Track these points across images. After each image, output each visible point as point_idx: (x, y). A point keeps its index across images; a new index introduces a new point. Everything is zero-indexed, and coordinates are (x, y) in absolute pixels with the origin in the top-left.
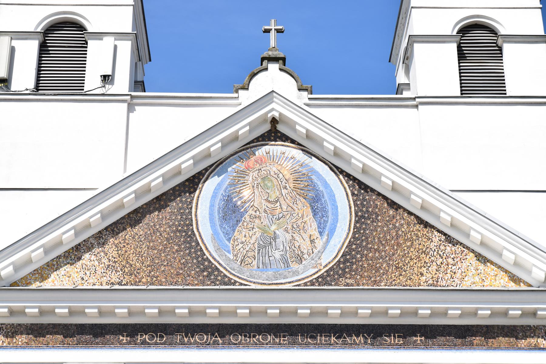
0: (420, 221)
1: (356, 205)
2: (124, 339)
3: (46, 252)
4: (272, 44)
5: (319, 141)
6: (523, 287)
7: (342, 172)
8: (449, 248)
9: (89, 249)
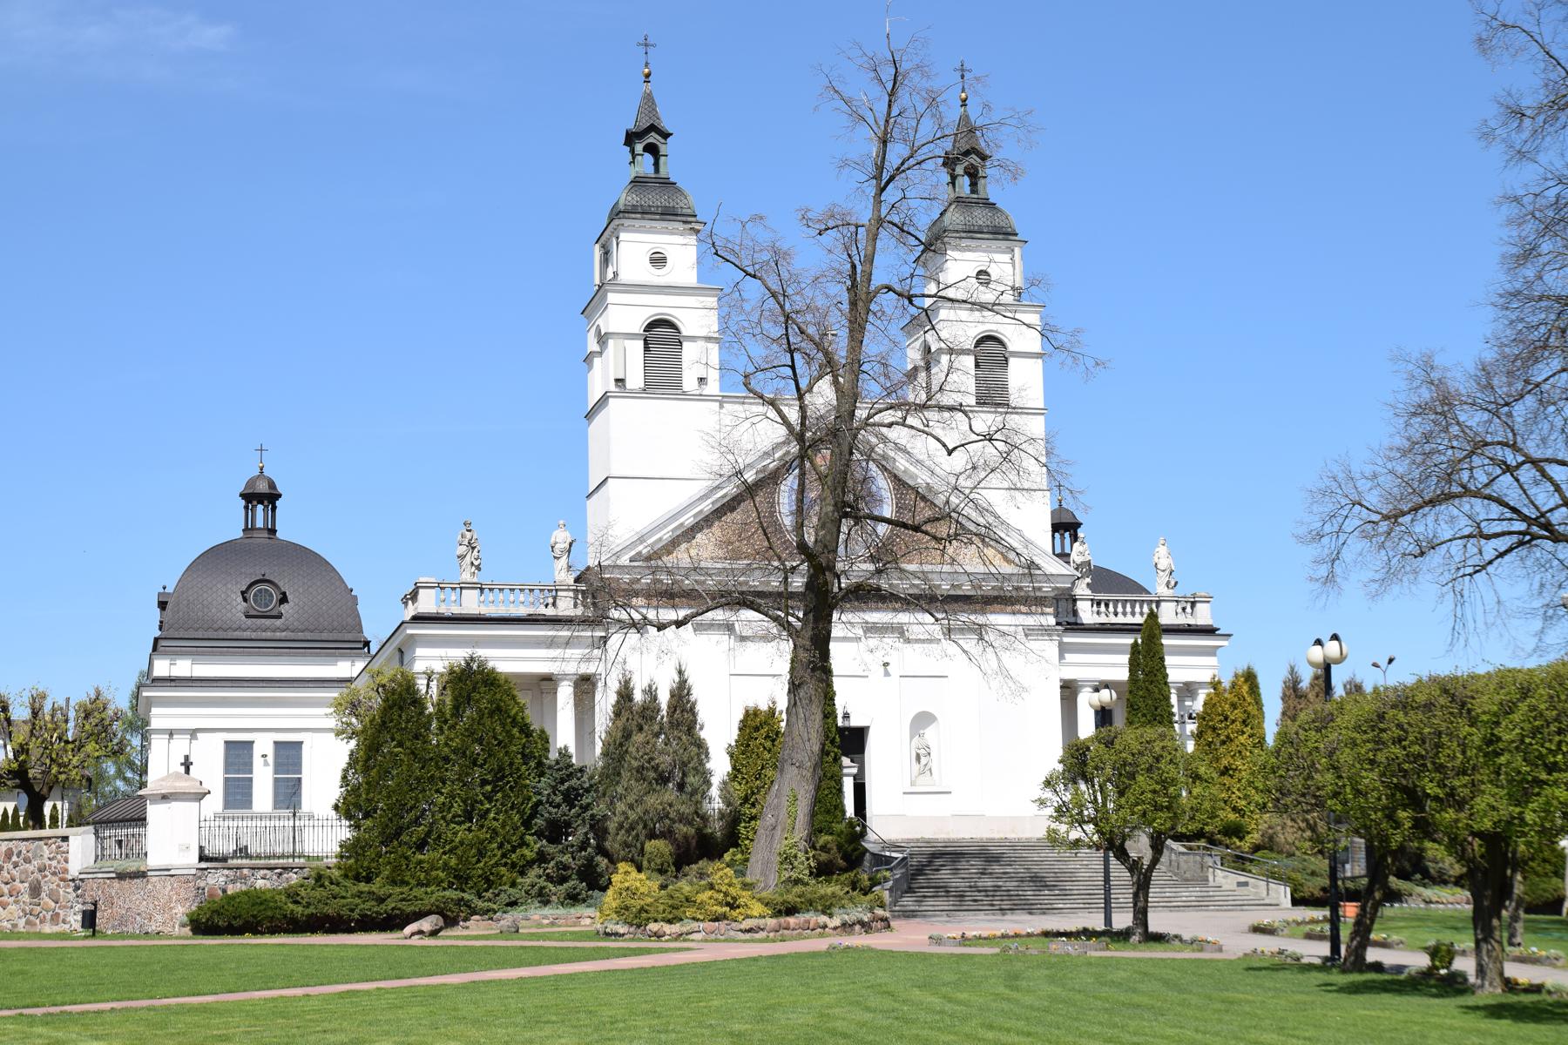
1: (896, 498)
9: (701, 530)
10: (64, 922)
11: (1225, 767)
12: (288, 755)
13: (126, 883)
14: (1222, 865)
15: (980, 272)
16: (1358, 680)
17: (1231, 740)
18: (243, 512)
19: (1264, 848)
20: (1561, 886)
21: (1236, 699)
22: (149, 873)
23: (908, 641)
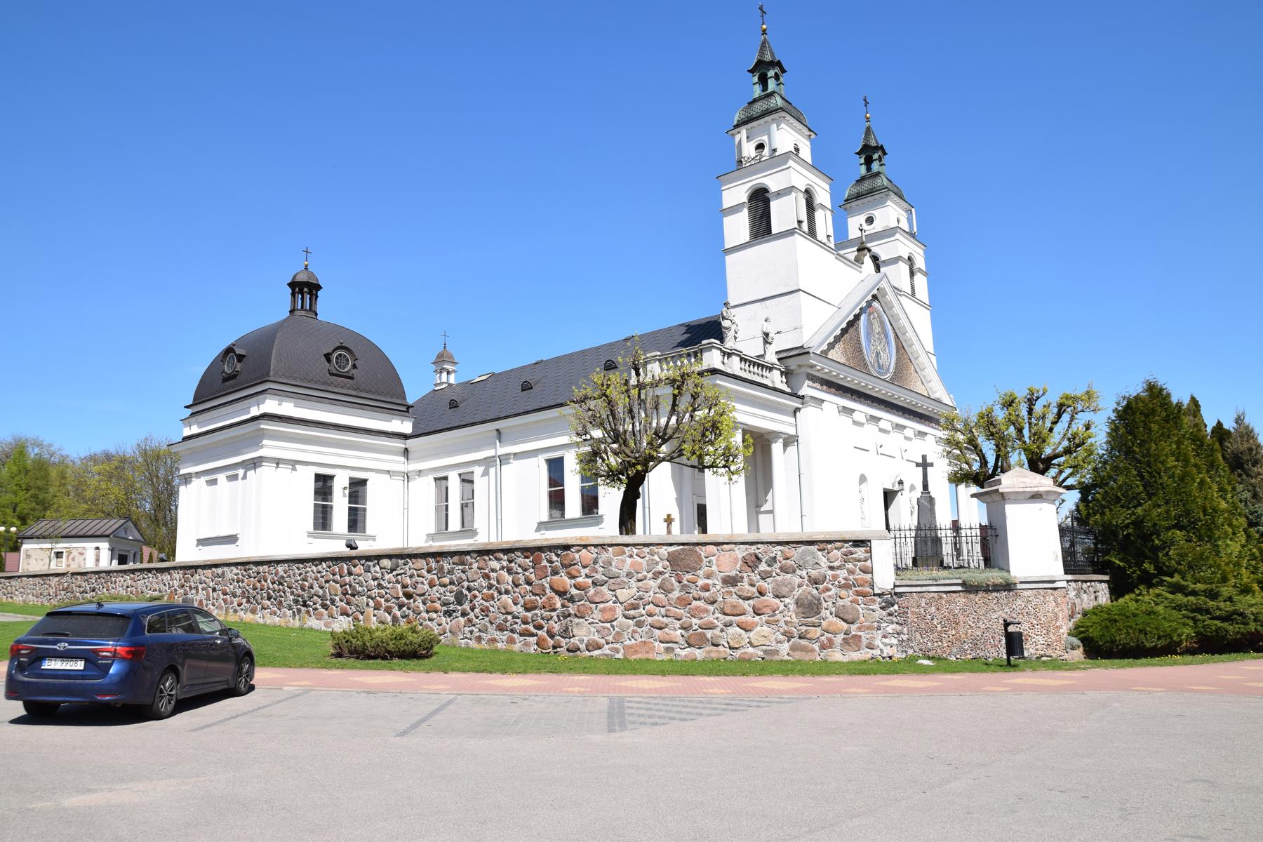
10: (870, 647)
12: (357, 488)
13: (978, 598)
18: (290, 297)
22: (1019, 586)
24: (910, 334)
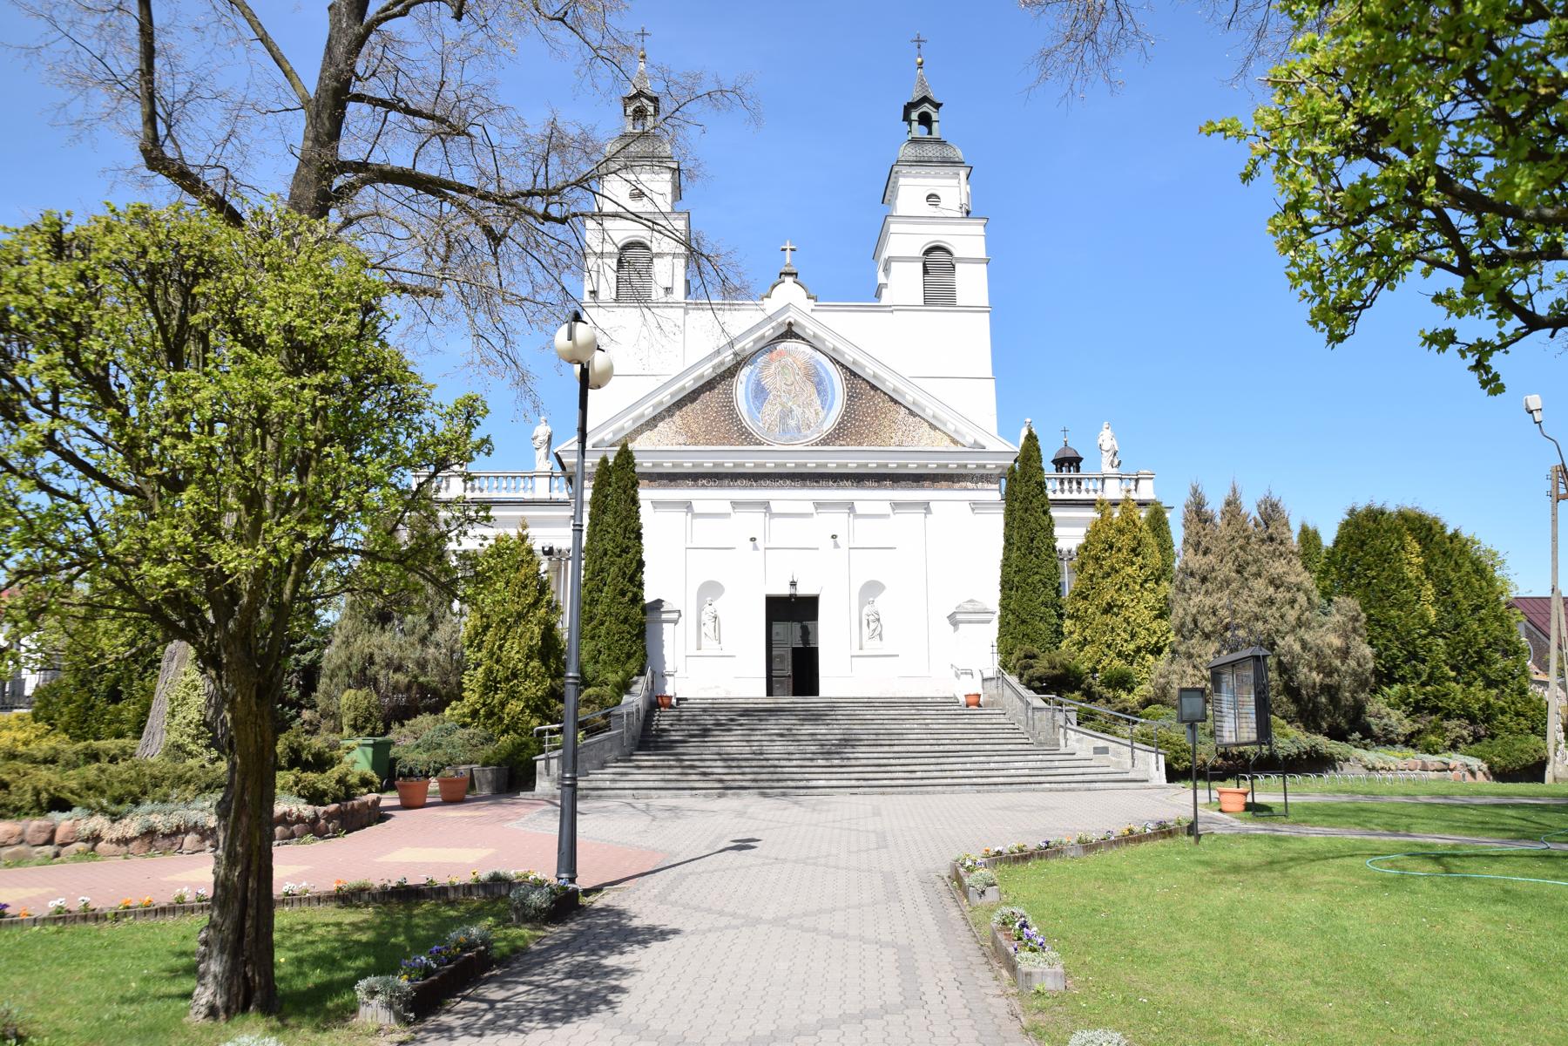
0: (892, 399)
2: (690, 483)
3: (634, 422)
4: (788, 260)
5: (823, 341)
6: (960, 448)
7: (838, 362)
8: (911, 419)
9: (663, 419)
11: (1108, 604)
14: (1079, 724)
15: (929, 197)
16: (1275, 499)
17: (1117, 572)
19: (1157, 702)
20: (1542, 745)
21: (1124, 524)
23: (857, 516)
24: (869, 370)
